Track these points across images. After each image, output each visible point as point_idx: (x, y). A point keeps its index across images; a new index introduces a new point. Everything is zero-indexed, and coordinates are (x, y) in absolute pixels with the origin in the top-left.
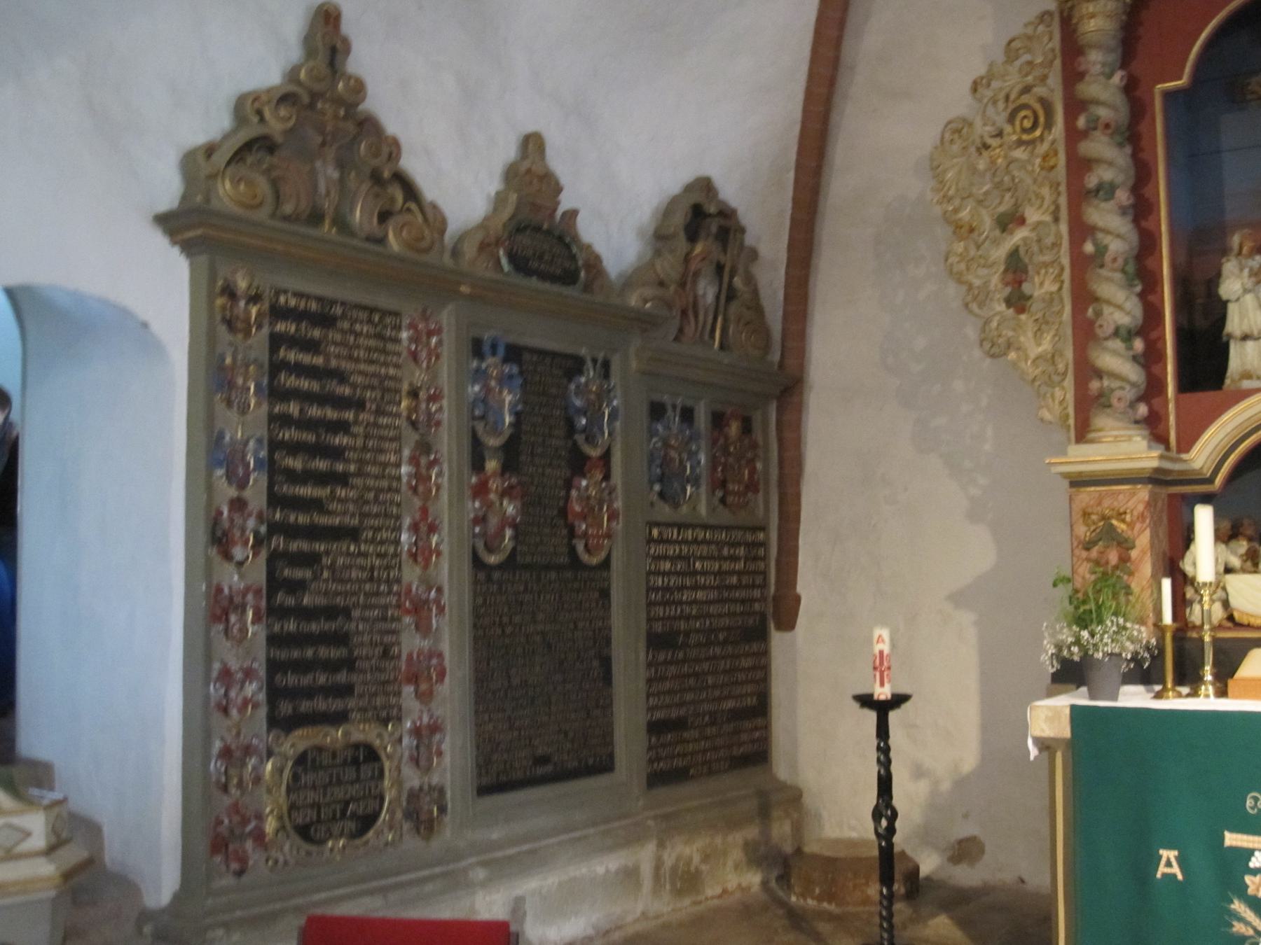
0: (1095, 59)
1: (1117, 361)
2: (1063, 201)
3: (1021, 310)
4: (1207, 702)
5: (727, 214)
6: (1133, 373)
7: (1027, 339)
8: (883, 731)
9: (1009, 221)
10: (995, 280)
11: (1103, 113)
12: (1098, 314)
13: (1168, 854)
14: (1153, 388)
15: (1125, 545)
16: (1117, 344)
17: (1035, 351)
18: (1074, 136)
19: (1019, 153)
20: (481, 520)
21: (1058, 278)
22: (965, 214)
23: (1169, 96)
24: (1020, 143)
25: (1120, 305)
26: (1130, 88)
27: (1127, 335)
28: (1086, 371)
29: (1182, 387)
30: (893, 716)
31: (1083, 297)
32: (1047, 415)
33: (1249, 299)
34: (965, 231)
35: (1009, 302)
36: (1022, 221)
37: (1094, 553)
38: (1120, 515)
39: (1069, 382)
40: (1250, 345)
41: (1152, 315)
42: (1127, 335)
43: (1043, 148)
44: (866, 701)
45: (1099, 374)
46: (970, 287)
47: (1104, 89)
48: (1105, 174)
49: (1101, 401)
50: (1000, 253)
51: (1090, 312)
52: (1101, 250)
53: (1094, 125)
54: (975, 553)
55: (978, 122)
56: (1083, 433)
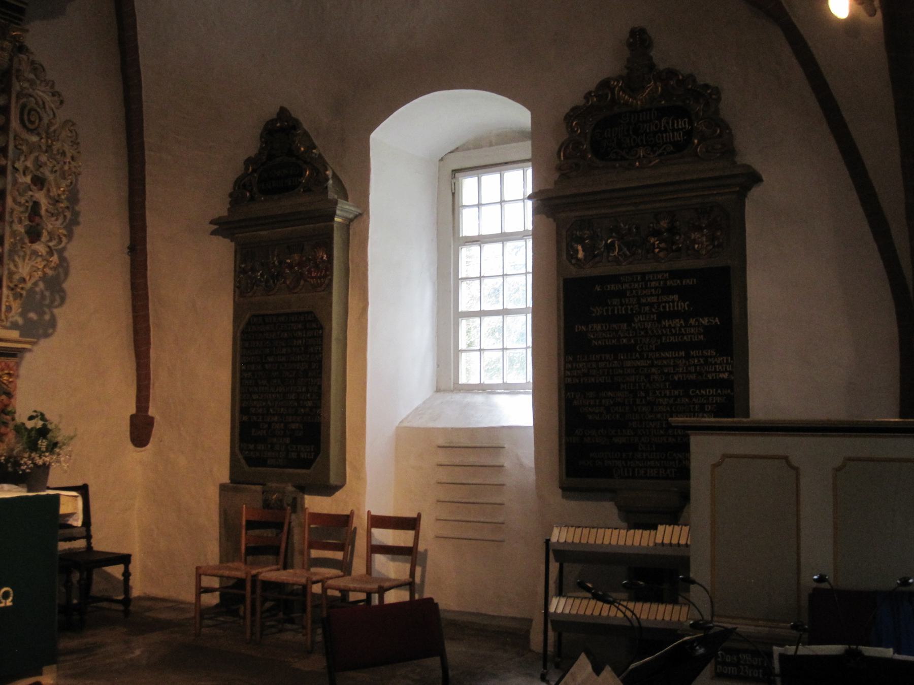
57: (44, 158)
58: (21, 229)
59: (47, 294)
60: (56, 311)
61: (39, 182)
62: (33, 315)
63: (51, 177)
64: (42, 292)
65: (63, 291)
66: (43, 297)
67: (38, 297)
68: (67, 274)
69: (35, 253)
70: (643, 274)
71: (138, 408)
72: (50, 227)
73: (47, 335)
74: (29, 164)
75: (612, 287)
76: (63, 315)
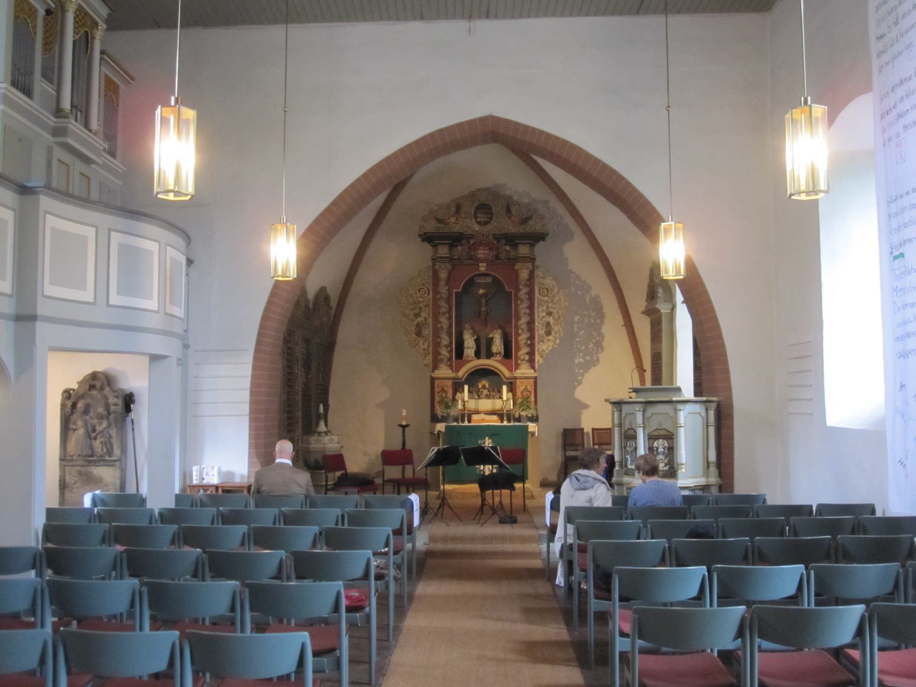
0: (442, 283)
7: (421, 344)
8: (404, 432)
9: (417, 315)
10: (413, 329)
14: (450, 359)
15: (446, 392)
17: (423, 347)
18: (435, 301)
19: (421, 299)
23: (456, 293)
26: (449, 290)
27: (446, 346)
28: (436, 354)
29: (456, 358)
30: (407, 429)
41: (451, 343)
42: (446, 346)
45: (440, 354)
47: (444, 290)
49: (441, 360)
50: (415, 323)
52: (442, 327)
53: (441, 298)
56: (435, 367)
58: (542, 332)
60: (600, 355)
61: (549, 314)
63: (555, 311)
68: (603, 337)
69: (549, 340)
73: (594, 365)
76: (603, 356)
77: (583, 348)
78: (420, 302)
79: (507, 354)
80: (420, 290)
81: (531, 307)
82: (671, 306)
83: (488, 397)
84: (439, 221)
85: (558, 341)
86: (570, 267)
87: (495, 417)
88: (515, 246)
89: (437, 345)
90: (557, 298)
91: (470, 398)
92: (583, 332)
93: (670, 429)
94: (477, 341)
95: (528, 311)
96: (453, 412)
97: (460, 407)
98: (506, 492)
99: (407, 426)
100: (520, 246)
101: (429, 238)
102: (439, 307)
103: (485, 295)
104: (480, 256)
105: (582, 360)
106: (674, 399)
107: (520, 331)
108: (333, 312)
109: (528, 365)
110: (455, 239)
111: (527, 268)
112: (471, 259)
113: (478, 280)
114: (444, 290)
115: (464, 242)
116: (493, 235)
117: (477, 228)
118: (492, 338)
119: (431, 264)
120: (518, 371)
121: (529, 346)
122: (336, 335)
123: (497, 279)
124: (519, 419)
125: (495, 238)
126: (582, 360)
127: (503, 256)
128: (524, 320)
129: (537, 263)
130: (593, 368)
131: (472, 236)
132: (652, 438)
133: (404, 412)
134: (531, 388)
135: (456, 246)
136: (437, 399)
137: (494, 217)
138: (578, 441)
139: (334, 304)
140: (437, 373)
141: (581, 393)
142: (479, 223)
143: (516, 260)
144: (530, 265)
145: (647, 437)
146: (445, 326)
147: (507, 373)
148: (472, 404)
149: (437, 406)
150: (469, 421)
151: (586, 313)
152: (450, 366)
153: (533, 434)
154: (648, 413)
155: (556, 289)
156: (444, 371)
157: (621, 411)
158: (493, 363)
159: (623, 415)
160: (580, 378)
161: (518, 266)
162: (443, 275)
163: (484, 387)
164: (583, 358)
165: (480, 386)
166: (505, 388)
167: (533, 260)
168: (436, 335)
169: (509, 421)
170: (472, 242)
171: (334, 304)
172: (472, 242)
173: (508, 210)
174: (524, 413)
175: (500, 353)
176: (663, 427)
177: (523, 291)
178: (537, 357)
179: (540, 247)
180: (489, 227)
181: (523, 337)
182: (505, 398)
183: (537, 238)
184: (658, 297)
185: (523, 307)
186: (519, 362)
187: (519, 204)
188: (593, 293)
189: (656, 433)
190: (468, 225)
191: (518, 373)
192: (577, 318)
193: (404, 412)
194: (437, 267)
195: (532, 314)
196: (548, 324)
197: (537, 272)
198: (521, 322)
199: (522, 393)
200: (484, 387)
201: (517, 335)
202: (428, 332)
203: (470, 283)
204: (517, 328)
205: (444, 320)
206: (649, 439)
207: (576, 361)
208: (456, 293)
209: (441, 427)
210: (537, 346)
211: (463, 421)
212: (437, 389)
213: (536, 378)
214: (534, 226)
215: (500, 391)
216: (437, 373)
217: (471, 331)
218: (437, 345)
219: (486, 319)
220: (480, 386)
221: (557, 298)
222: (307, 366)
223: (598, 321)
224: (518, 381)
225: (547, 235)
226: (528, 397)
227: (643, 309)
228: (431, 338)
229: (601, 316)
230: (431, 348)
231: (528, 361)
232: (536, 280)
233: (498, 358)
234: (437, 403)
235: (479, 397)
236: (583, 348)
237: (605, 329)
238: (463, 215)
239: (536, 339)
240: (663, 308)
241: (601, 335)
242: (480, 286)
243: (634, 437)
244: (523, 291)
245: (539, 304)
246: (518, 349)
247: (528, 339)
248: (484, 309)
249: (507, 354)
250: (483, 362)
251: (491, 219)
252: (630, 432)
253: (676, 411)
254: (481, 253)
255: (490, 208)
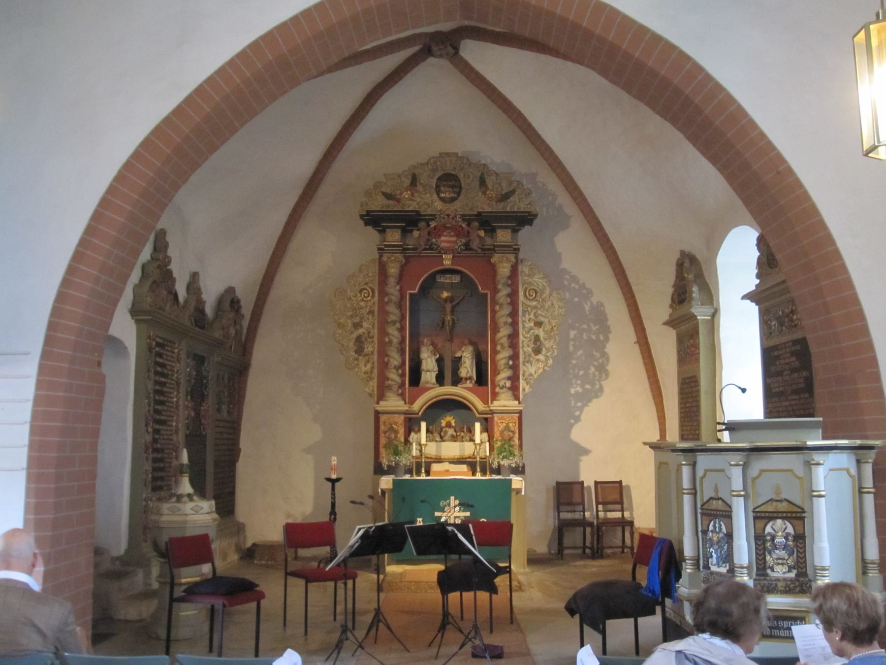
0: (392, 281)
1: (394, 376)
2: (376, 322)
3: (360, 355)
4: (423, 477)
5: (238, 301)
6: (398, 380)
7: (362, 365)
8: (333, 489)
9: (357, 326)
10: (351, 344)
11: (393, 298)
12: (389, 361)
13: (419, 519)
14: (402, 385)
15: (396, 432)
16: (394, 371)
17: (364, 369)
18: (382, 304)
19: (362, 304)
20: (187, 418)
21: (373, 347)
22: (342, 321)
23: (411, 295)
24: (363, 300)
25: (395, 359)
26: (401, 290)
28: (383, 379)
29: (410, 385)
30: (337, 484)
31: (383, 353)
32: (367, 389)
33: (429, 359)
34: (340, 325)
35: (356, 352)
36: (362, 327)
37: (387, 435)
38: (396, 424)
39: (375, 380)
40: (428, 373)
41: (404, 362)
43: (370, 304)
44: (329, 480)
45: (388, 379)
46: (343, 345)
47: (393, 290)
48: (392, 318)
49: (389, 388)
50: (354, 335)
51: (386, 359)
52: (391, 342)
53: (390, 301)
54: (315, 433)
55: (349, 291)
56: (381, 397)
57: (539, 312)
59: (597, 373)
60: (603, 383)
61: (539, 324)
62: (588, 387)
63: (546, 321)
64: (593, 373)
65: (607, 371)
66: (594, 376)
67: (591, 376)
68: (608, 360)
69: (538, 360)
70: (784, 343)
71: (661, 437)
72: (547, 346)
73: (597, 397)
74: (532, 316)
75: (776, 353)
77: (581, 373)
78: (362, 308)
79: (481, 379)
80: (361, 291)
81: (514, 314)
82: (713, 311)
83: (454, 439)
84: (388, 196)
85: (551, 362)
86: (565, 265)
87: (464, 468)
88: (491, 231)
89: (384, 366)
90: (549, 303)
91: (429, 440)
92: (580, 352)
93: (798, 502)
94: (440, 362)
95: (510, 320)
96: (404, 460)
97: (415, 452)
98: (483, 596)
99: (338, 480)
100: (499, 231)
101: (374, 220)
102: (388, 313)
103: (451, 299)
104: (443, 245)
105: (580, 390)
106: (810, 443)
107: (499, 348)
108: (245, 323)
109: (510, 393)
110: (410, 221)
111: (508, 260)
112: (432, 249)
113: (441, 279)
114: (393, 290)
115: (422, 224)
116: (463, 215)
117: (439, 205)
118: (460, 358)
119: (377, 256)
120: (495, 403)
121: (511, 367)
122: (251, 354)
123: (467, 275)
124: (498, 471)
125: (464, 220)
126: (580, 390)
127: (475, 245)
128: (504, 332)
129: (521, 255)
130: (595, 400)
131: (433, 217)
132: (761, 517)
133: (334, 461)
134: (514, 427)
135: (411, 231)
136: (383, 441)
137: (463, 191)
138: (577, 499)
139: (247, 310)
140: (384, 406)
141: (578, 434)
142: (443, 200)
143: (493, 249)
144: (512, 257)
145: (751, 515)
146: (395, 341)
147: (480, 405)
148: (431, 449)
149: (383, 451)
150: (428, 473)
151: (585, 326)
152: (402, 395)
153: (518, 491)
154: (754, 472)
155: (548, 291)
156: (393, 403)
157: (694, 465)
158: (463, 392)
159: (700, 473)
160: (577, 413)
161: (495, 259)
162: (393, 270)
163: (449, 425)
164: (582, 386)
165: (444, 424)
166: (478, 426)
167: (516, 250)
168: (383, 353)
169: (484, 472)
170: (433, 224)
171: (247, 310)
172: (433, 224)
173: (482, 182)
174: (505, 463)
175: (470, 378)
176: (783, 496)
177: (503, 293)
178: (522, 384)
179: (525, 231)
180: (457, 204)
181: (503, 355)
182: (478, 441)
183: (525, 219)
184: (691, 299)
185: (503, 315)
186: (497, 390)
187: (497, 175)
188: (594, 300)
189: (770, 508)
190: (428, 201)
191: (496, 405)
192: (572, 333)
193: (334, 461)
194: (385, 259)
195: (514, 324)
196: (537, 338)
197: (523, 269)
198: (499, 335)
199: (502, 433)
200: (449, 425)
201: (495, 352)
202: (370, 348)
203: (429, 285)
204: (494, 343)
205: (393, 332)
206: (755, 518)
207: (573, 391)
208: (411, 295)
209: (386, 482)
210: (522, 368)
211: (419, 473)
212: (382, 428)
213: (520, 412)
214: (517, 204)
215: (471, 431)
216: (384, 406)
217: (431, 348)
218: (384, 366)
219: (451, 331)
220: (444, 424)
221: (549, 303)
222: (197, 393)
223: (602, 338)
224: (496, 417)
225: (536, 216)
226: (511, 439)
227: (666, 317)
228: (376, 357)
229: (605, 330)
230: (375, 371)
231: (509, 389)
232: (520, 277)
233: (469, 384)
234: (383, 446)
235: (442, 439)
236: (581, 373)
237: (611, 348)
238: (420, 188)
239: (521, 360)
240: (701, 313)
241: (604, 355)
242: (443, 287)
243: (727, 515)
244: (503, 293)
245: (524, 312)
246: (496, 372)
247: (510, 358)
248: (449, 318)
249: (481, 379)
250: (448, 390)
251: (459, 194)
252: (717, 505)
253: (809, 465)
254: (445, 240)
255: (459, 180)
